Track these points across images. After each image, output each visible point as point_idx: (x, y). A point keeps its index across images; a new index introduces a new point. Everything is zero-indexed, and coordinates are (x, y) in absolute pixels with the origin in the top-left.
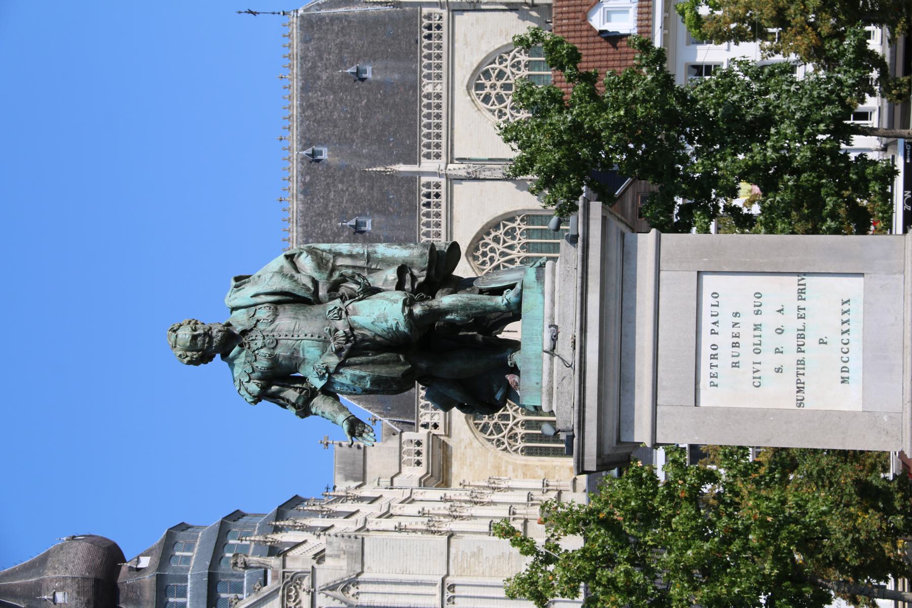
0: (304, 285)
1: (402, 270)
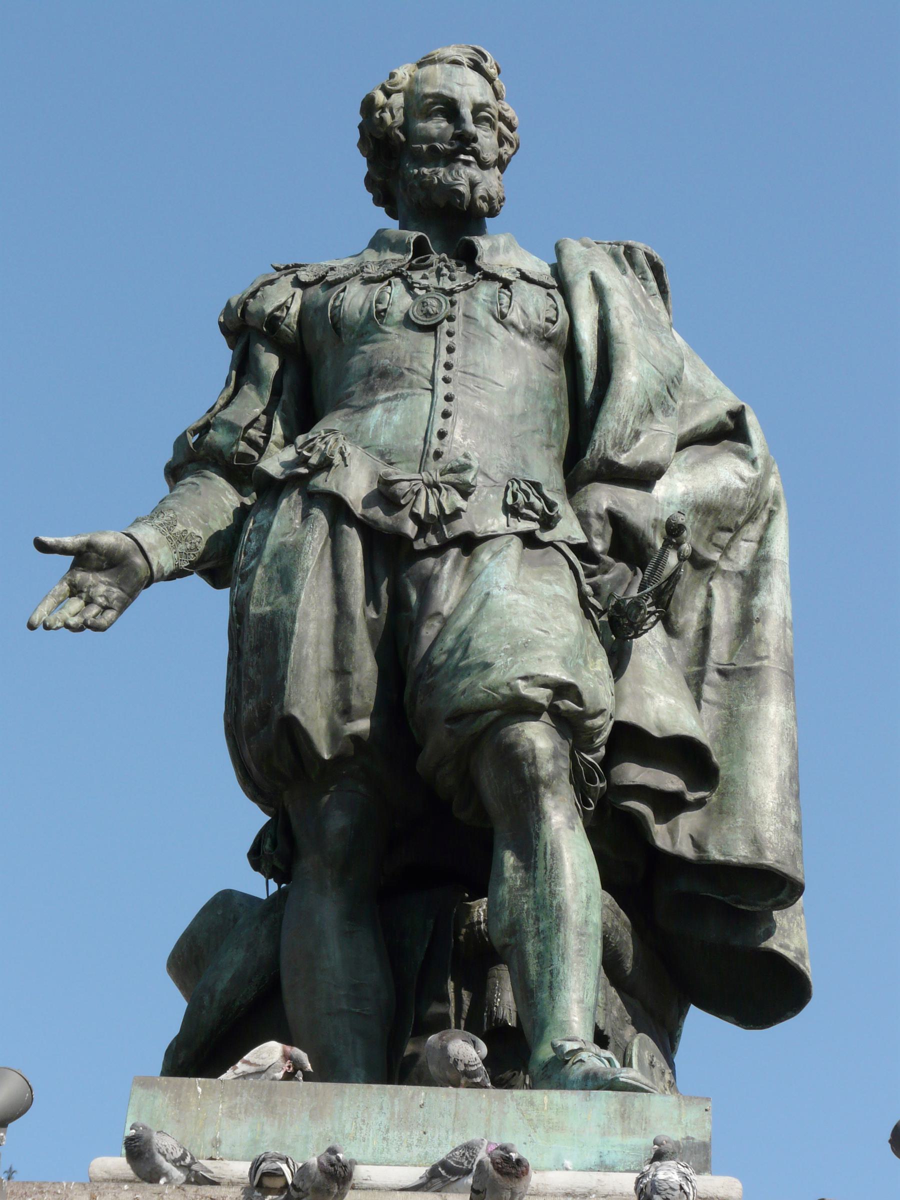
0: (637, 435)
1: (692, 759)
